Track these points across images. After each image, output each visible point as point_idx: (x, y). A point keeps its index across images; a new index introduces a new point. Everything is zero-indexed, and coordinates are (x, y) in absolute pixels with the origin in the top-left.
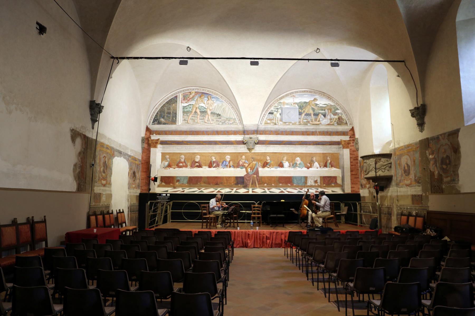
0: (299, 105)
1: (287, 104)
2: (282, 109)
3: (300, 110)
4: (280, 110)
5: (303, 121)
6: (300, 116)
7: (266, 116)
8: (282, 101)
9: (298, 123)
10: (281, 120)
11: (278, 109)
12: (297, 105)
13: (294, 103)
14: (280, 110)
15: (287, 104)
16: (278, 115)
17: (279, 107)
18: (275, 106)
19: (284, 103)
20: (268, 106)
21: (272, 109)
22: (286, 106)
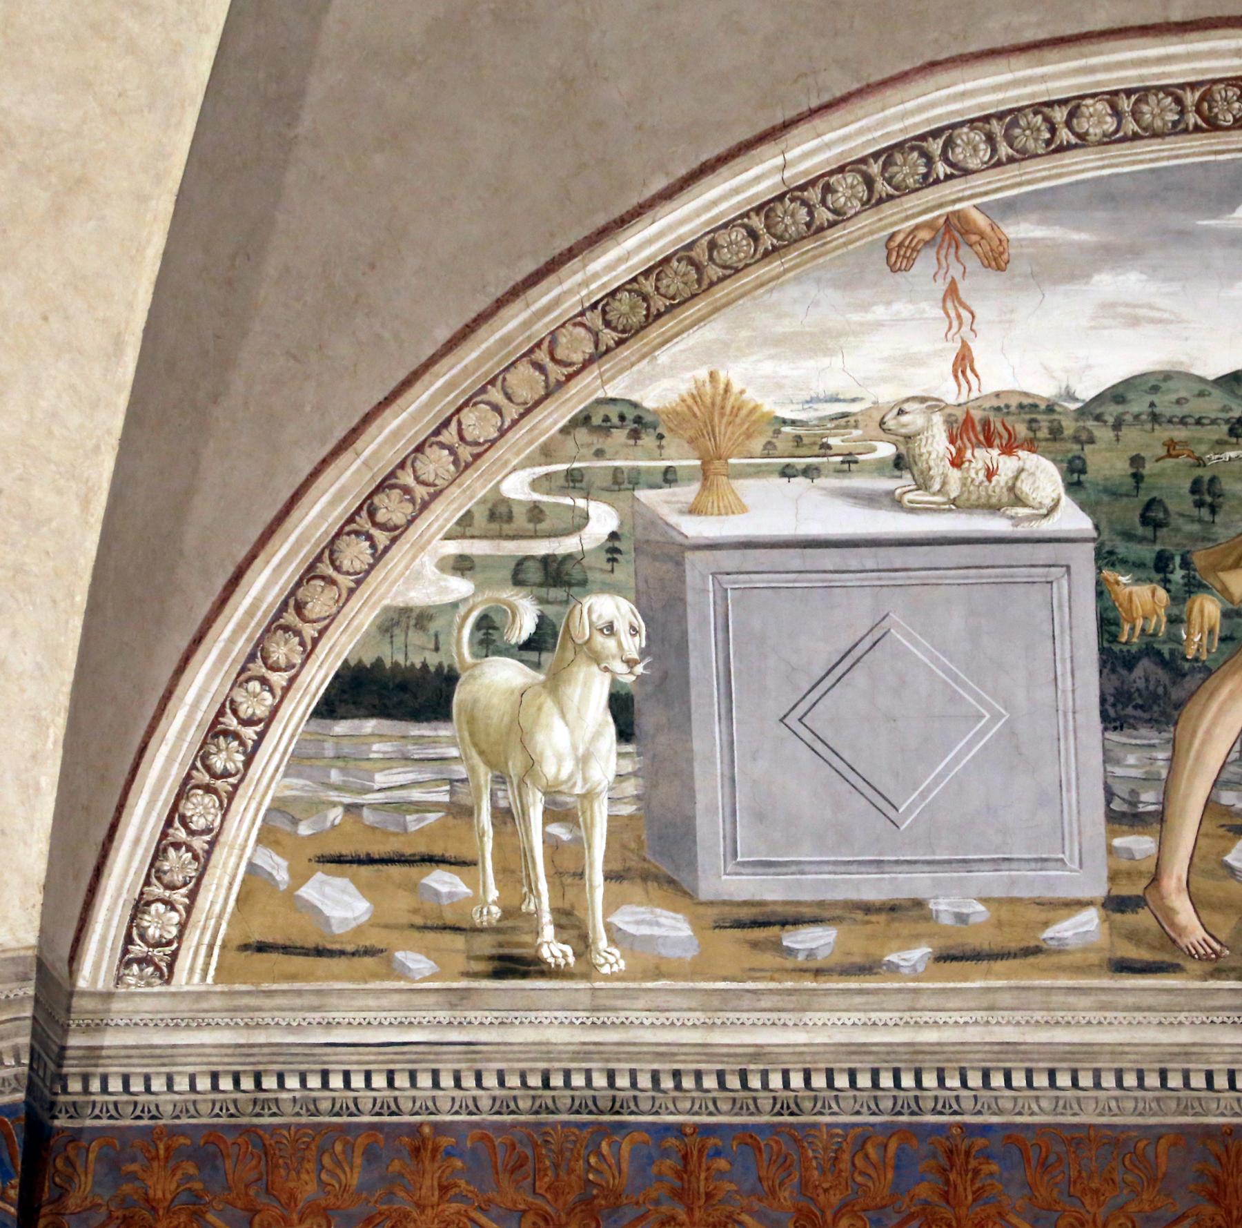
0: (1108, 463)
1: (803, 451)
2: (655, 566)
3: (1144, 599)
4: (609, 609)
5: (1208, 867)
6: (1139, 756)
7: (267, 779)
8: (660, 378)
9: (1083, 928)
10: (656, 857)
11: (557, 576)
12: (1043, 477)
13: (978, 429)
14: (609, 609)
15: (803, 451)
16: (576, 741)
17: (603, 520)
18: (499, 515)
19: (716, 435)
20: (320, 514)
21: (423, 574)
22: (775, 508)
